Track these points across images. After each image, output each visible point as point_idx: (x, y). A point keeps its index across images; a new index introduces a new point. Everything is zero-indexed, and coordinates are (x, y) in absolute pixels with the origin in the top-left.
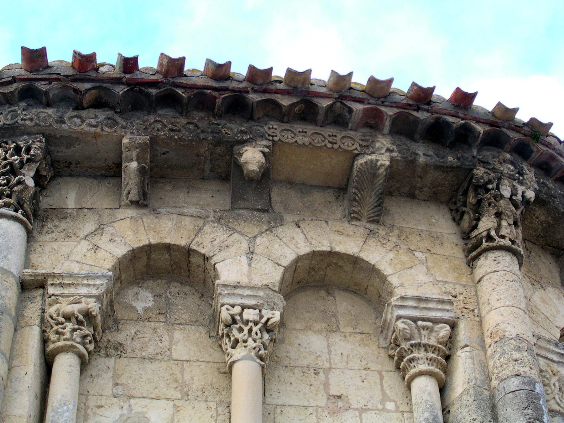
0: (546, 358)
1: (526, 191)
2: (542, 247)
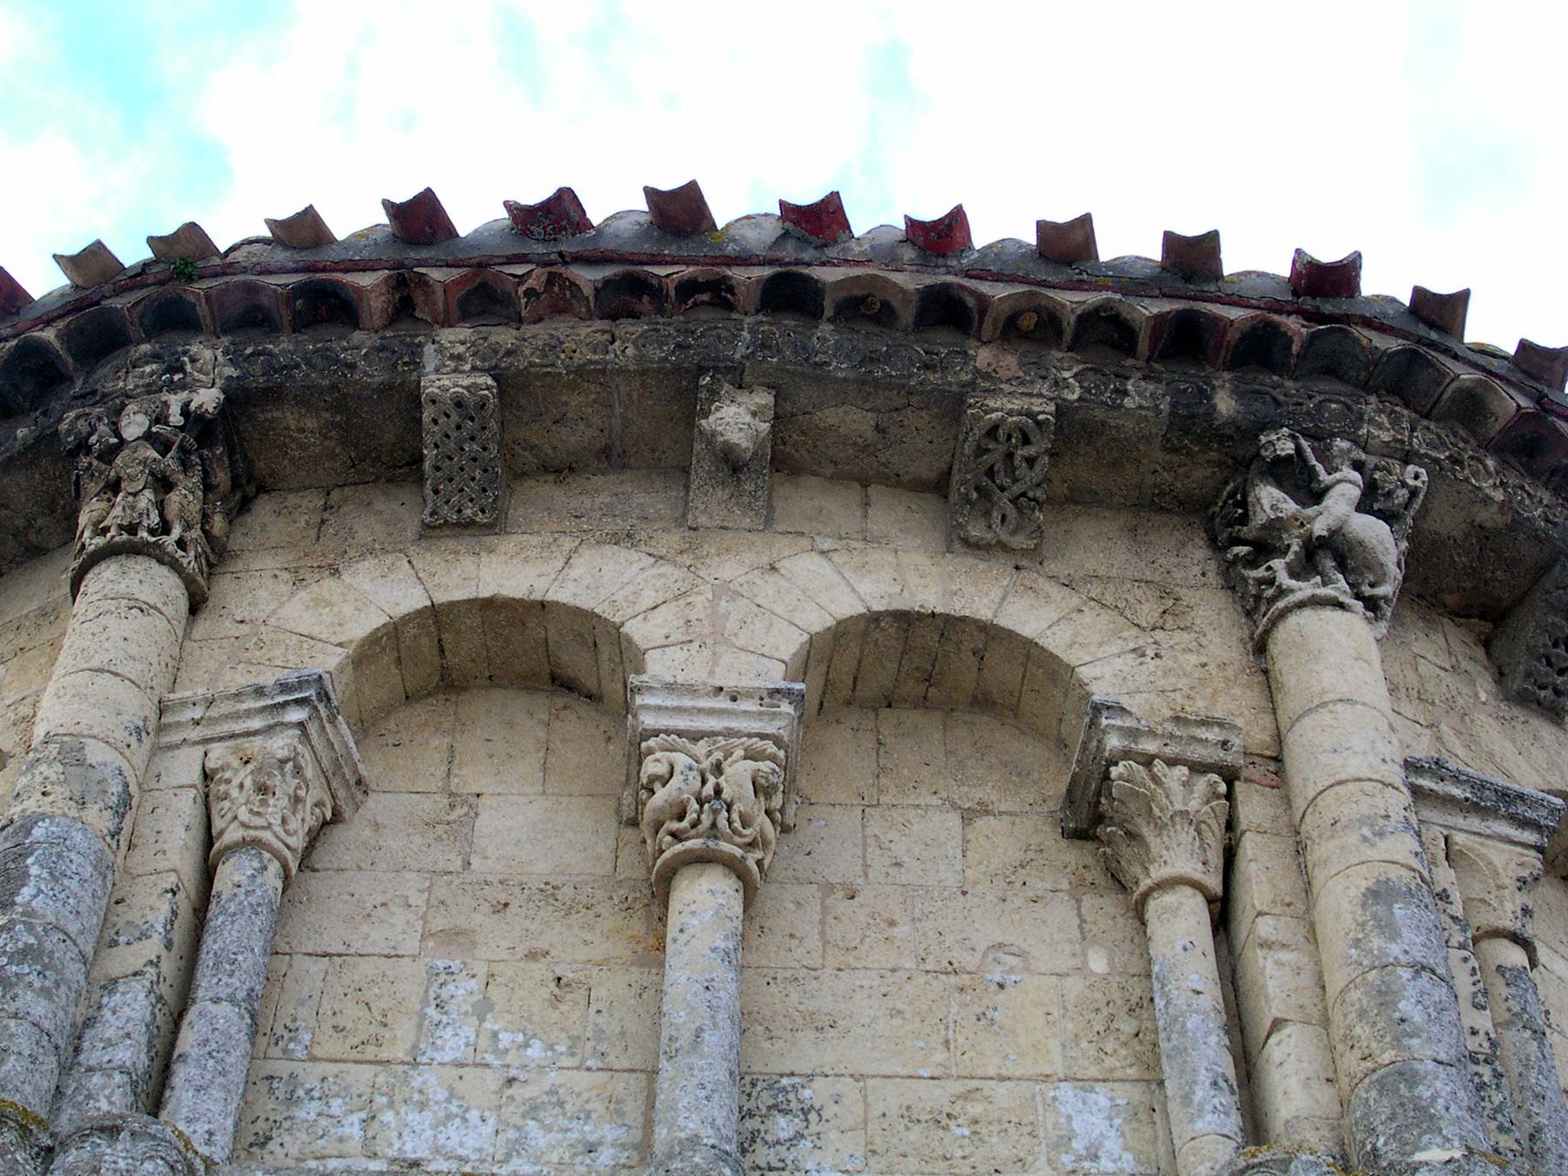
0: (233, 736)
2: (388, 481)
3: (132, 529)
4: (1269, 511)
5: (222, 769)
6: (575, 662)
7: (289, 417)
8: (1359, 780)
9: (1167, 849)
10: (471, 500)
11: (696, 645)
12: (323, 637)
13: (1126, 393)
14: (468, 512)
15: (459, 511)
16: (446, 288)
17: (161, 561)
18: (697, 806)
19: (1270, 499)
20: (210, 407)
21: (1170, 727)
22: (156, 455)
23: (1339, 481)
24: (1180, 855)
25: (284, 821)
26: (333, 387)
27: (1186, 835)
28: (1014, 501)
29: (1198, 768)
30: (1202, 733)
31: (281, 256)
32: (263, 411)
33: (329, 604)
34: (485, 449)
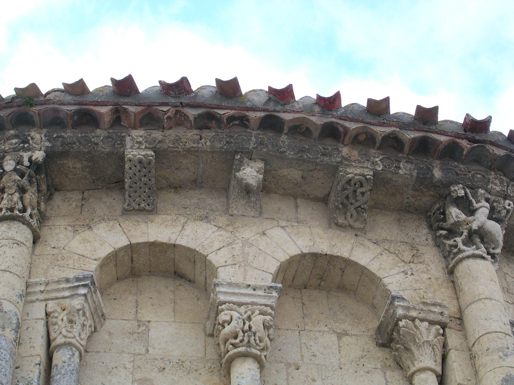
0: (57, 298)
1: (33, 154)
2: (108, 189)
3: (12, 210)
4: (455, 218)
5: (54, 312)
6: (185, 268)
7: (70, 163)
8: (496, 332)
9: (421, 355)
10: (144, 200)
11: (237, 266)
12: (88, 256)
13: (399, 168)
14: (143, 205)
15: (139, 205)
16: (135, 114)
17: (23, 223)
18: (242, 334)
19: (455, 213)
20: (40, 159)
21: (421, 306)
22: (19, 178)
23: (481, 207)
24: (426, 359)
25: (80, 334)
26: (89, 152)
27: (428, 350)
28: (356, 209)
29: (432, 323)
30: (433, 309)
31: (69, 98)
32: (60, 160)
33: (89, 242)
34: (150, 180)
